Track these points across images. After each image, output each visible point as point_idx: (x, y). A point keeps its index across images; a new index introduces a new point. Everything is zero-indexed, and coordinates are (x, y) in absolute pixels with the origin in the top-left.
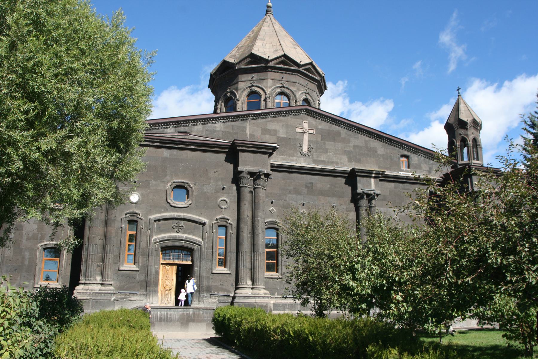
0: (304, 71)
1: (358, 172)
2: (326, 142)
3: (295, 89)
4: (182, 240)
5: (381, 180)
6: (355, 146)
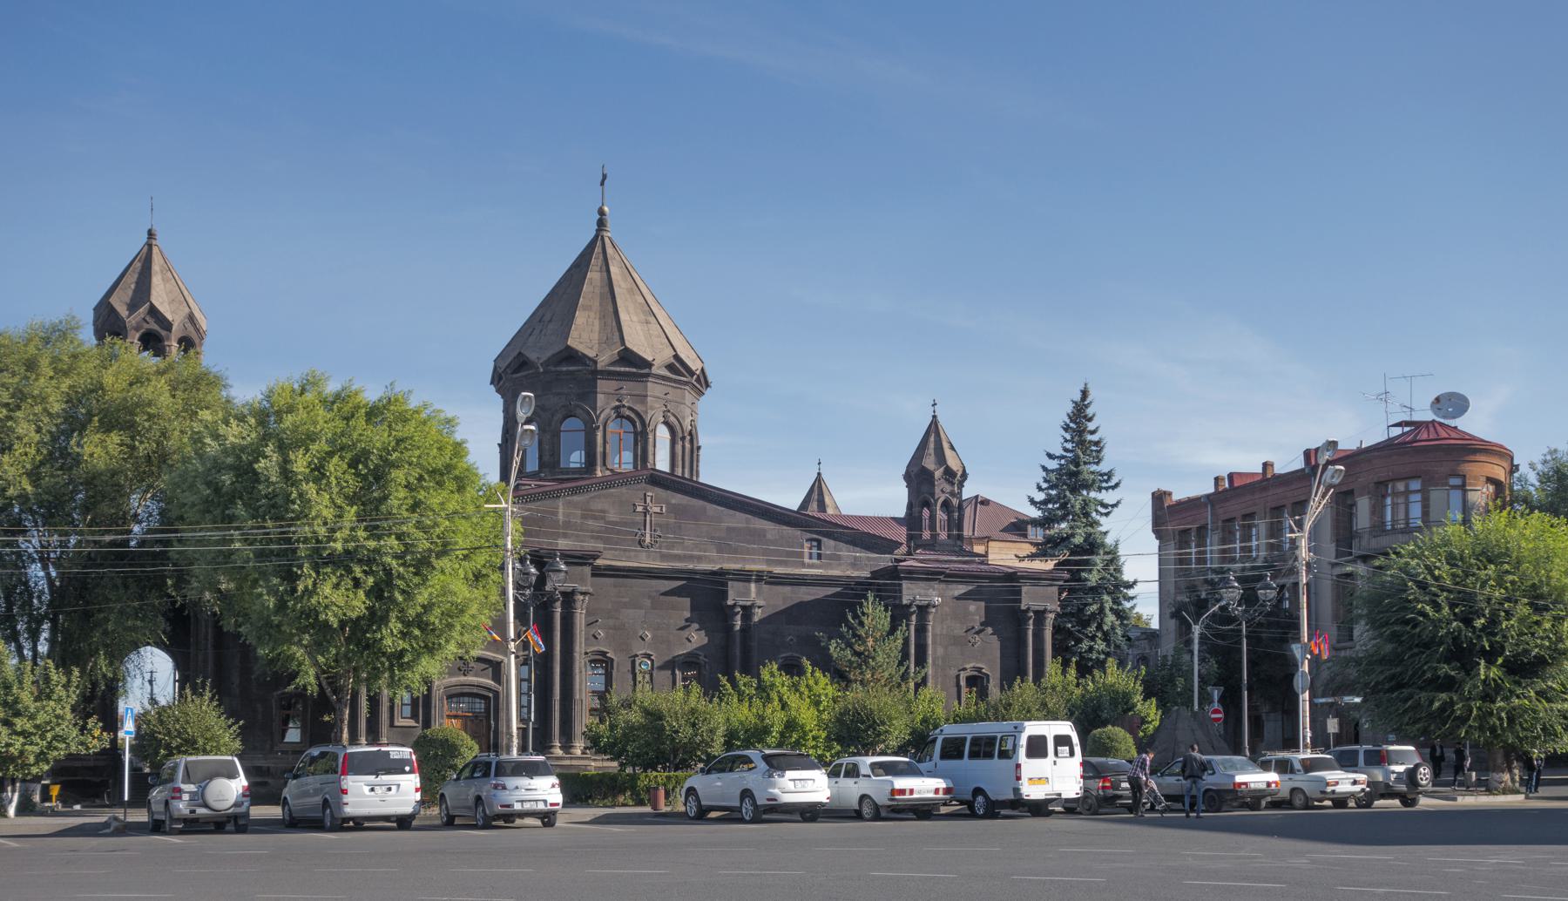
1: (729, 574)
3: (644, 409)
4: (473, 686)
5: (767, 583)
6: (729, 529)
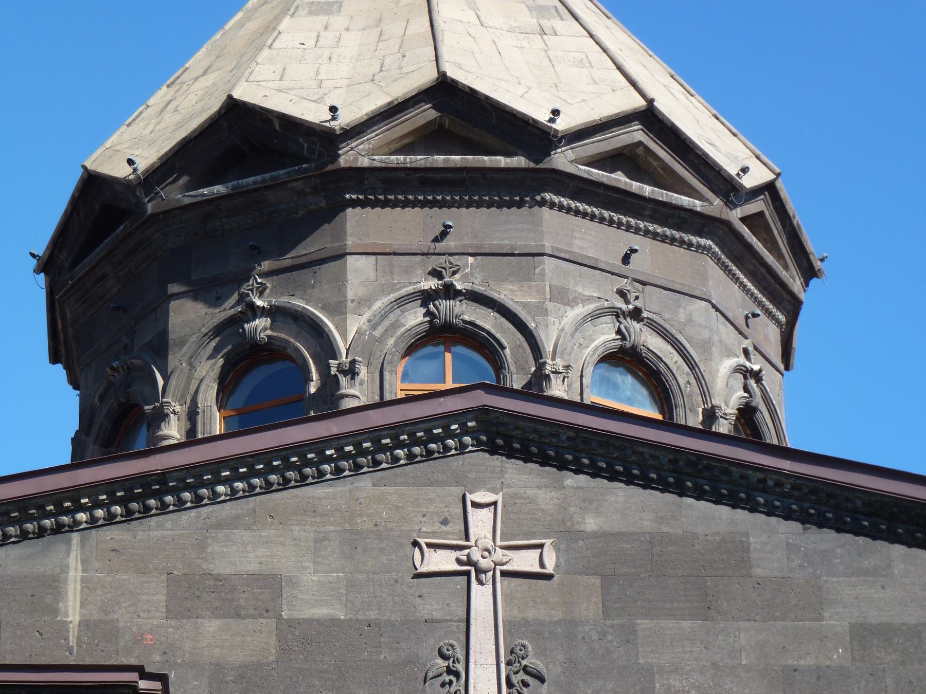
0: (596, 174)
2: (643, 624)
